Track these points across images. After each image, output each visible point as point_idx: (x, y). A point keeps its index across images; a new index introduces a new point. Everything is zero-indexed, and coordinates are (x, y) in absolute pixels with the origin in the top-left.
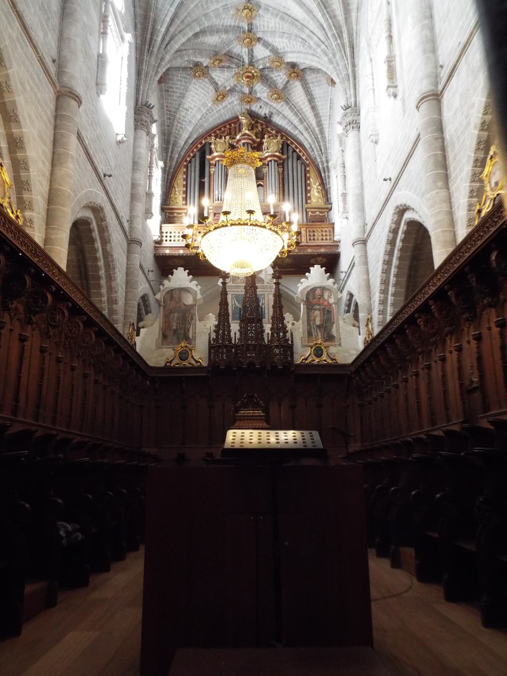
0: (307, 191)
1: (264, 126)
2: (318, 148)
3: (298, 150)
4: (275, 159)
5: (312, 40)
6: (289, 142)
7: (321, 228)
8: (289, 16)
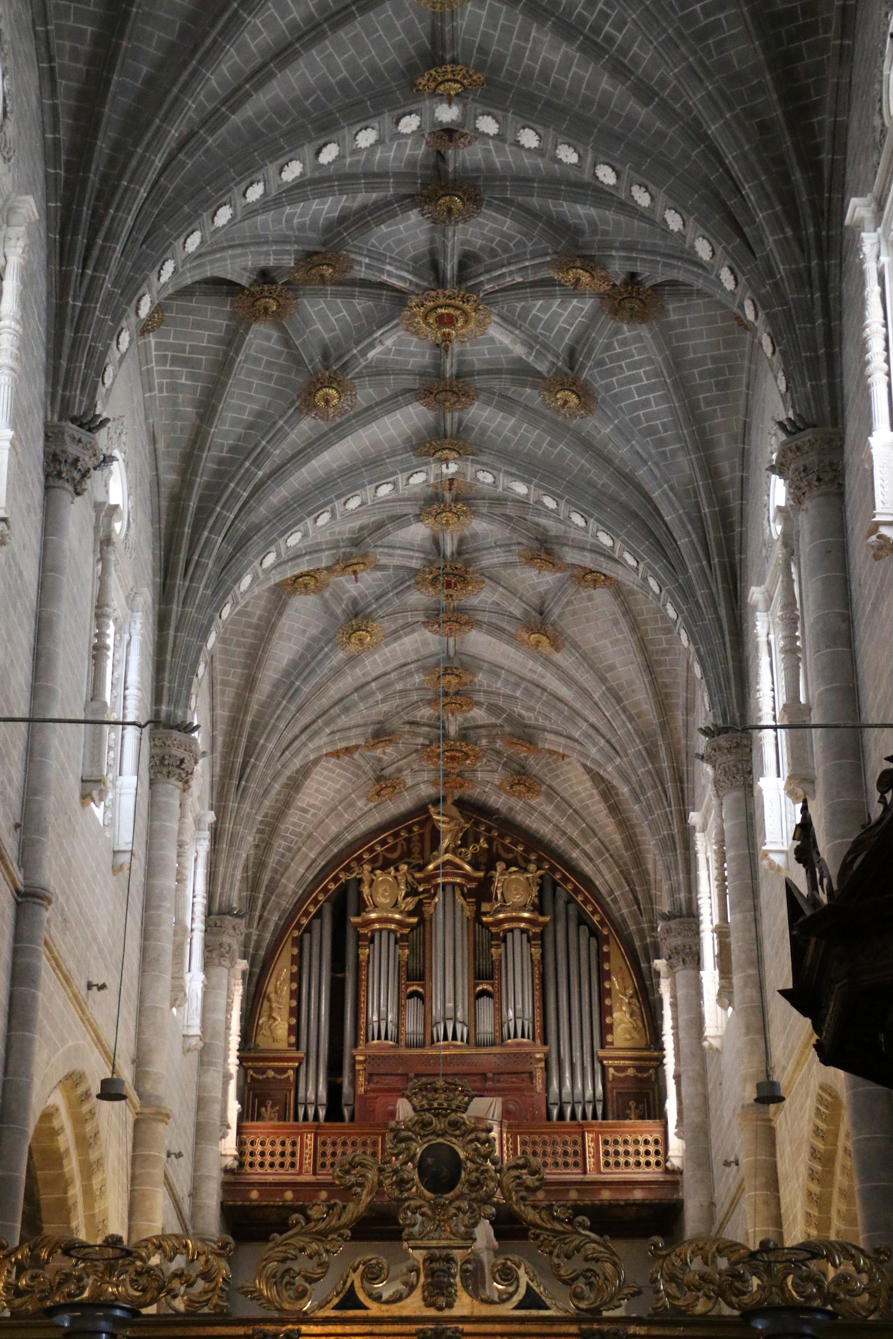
0: (605, 1011)
3: (580, 899)
4: (523, 925)
5: (595, 744)
6: (558, 876)
7: (635, 1132)
8: (544, 689)
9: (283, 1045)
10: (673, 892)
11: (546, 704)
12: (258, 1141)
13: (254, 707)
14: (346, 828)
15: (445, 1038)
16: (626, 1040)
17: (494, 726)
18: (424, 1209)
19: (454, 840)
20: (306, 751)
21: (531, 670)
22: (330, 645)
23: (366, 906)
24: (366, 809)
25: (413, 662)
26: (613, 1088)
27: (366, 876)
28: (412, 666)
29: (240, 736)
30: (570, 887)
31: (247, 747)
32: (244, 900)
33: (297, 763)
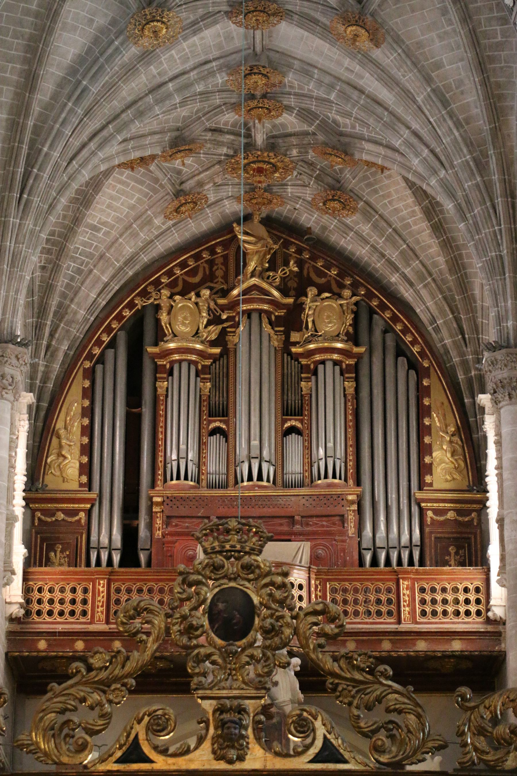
1: (306, 256)
2: (455, 325)
4: (335, 356)
5: (417, 154)
6: (375, 303)
7: (453, 580)
9: (75, 486)
10: (500, 320)
11: (365, 108)
12: (46, 588)
13: (36, 109)
14: (142, 249)
15: (250, 478)
16: (447, 481)
17: (306, 134)
18: (214, 658)
19: (262, 264)
20: (95, 160)
21: (347, 69)
22: (121, 38)
23: (165, 335)
24: (164, 227)
25: (215, 60)
26: (431, 533)
27: (164, 302)
28: (214, 64)
29: (21, 142)
30: (388, 315)
31: (29, 155)
32: (30, 329)
33: (85, 175)
